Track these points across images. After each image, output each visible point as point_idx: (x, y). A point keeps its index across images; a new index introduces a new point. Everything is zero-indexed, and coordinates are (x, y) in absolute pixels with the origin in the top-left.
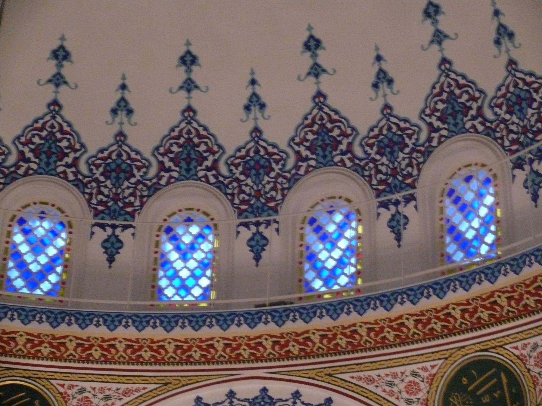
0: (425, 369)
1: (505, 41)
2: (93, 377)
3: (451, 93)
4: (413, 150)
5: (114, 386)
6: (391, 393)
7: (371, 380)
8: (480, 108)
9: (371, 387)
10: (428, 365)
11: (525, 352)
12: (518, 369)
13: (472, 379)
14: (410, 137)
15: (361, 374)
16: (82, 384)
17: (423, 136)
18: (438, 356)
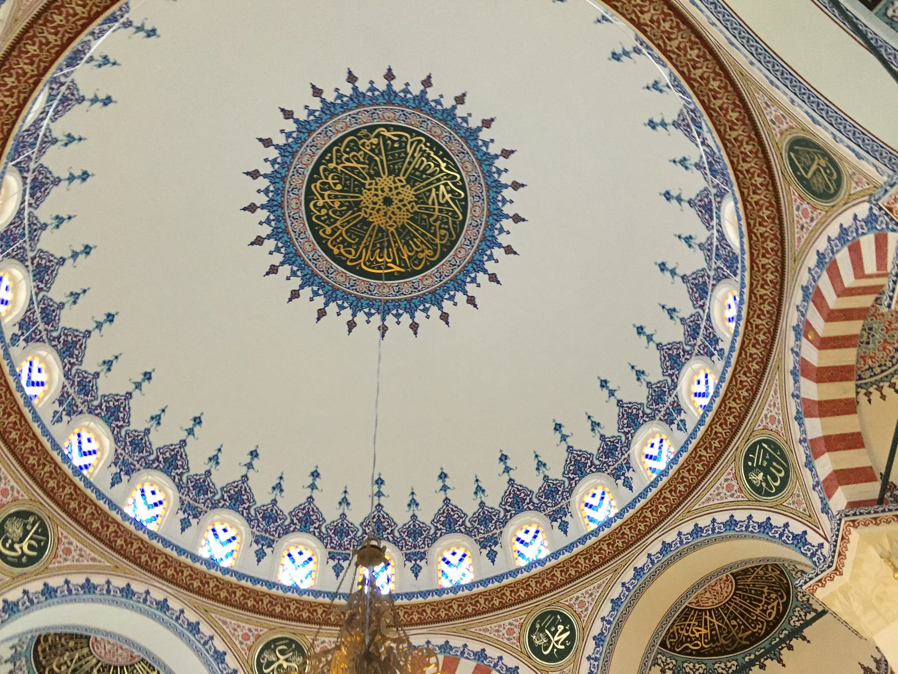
5: (592, 587)
7: (709, 499)
10: (729, 470)
11: (764, 424)
13: (752, 460)
15: (703, 500)
16: (575, 595)
18: (730, 463)
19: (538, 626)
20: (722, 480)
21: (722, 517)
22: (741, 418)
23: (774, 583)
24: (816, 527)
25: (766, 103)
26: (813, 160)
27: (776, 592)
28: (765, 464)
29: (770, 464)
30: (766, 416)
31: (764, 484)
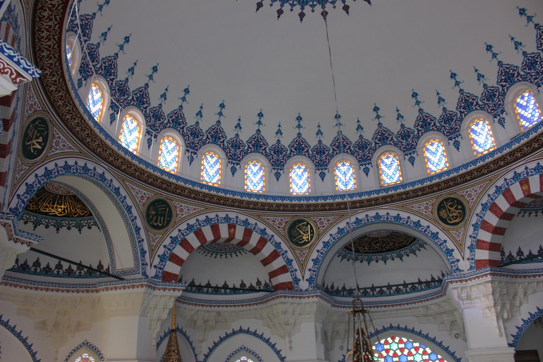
0: (148, 194)
1: (199, 116)
2: (65, 135)
3: (178, 116)
4: (161, 123)
5: (68, 143)
6: (136, 196)
7: (133, 189)
8: (183, 127)
9: (132, 191)
10: (150, 193)
12: (173, 209)
13: (158, 205)
14: (163, 119)
16: (61, 135)
17: (166, 122)
19: (37, 123)
20: (144, 191)
21: (129, 202)
22: (179, 194)
23: (71, 210)
24: (152, 257)
25: (328, 221)
26: (304, 232)
27: (64, 211)
28: (160, 212)
29: (161, 215)
30: (181, 206)
31: (151, 216)
